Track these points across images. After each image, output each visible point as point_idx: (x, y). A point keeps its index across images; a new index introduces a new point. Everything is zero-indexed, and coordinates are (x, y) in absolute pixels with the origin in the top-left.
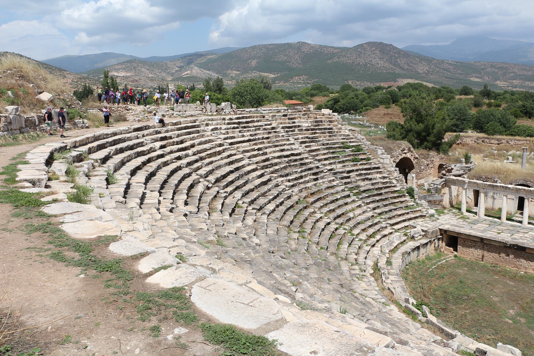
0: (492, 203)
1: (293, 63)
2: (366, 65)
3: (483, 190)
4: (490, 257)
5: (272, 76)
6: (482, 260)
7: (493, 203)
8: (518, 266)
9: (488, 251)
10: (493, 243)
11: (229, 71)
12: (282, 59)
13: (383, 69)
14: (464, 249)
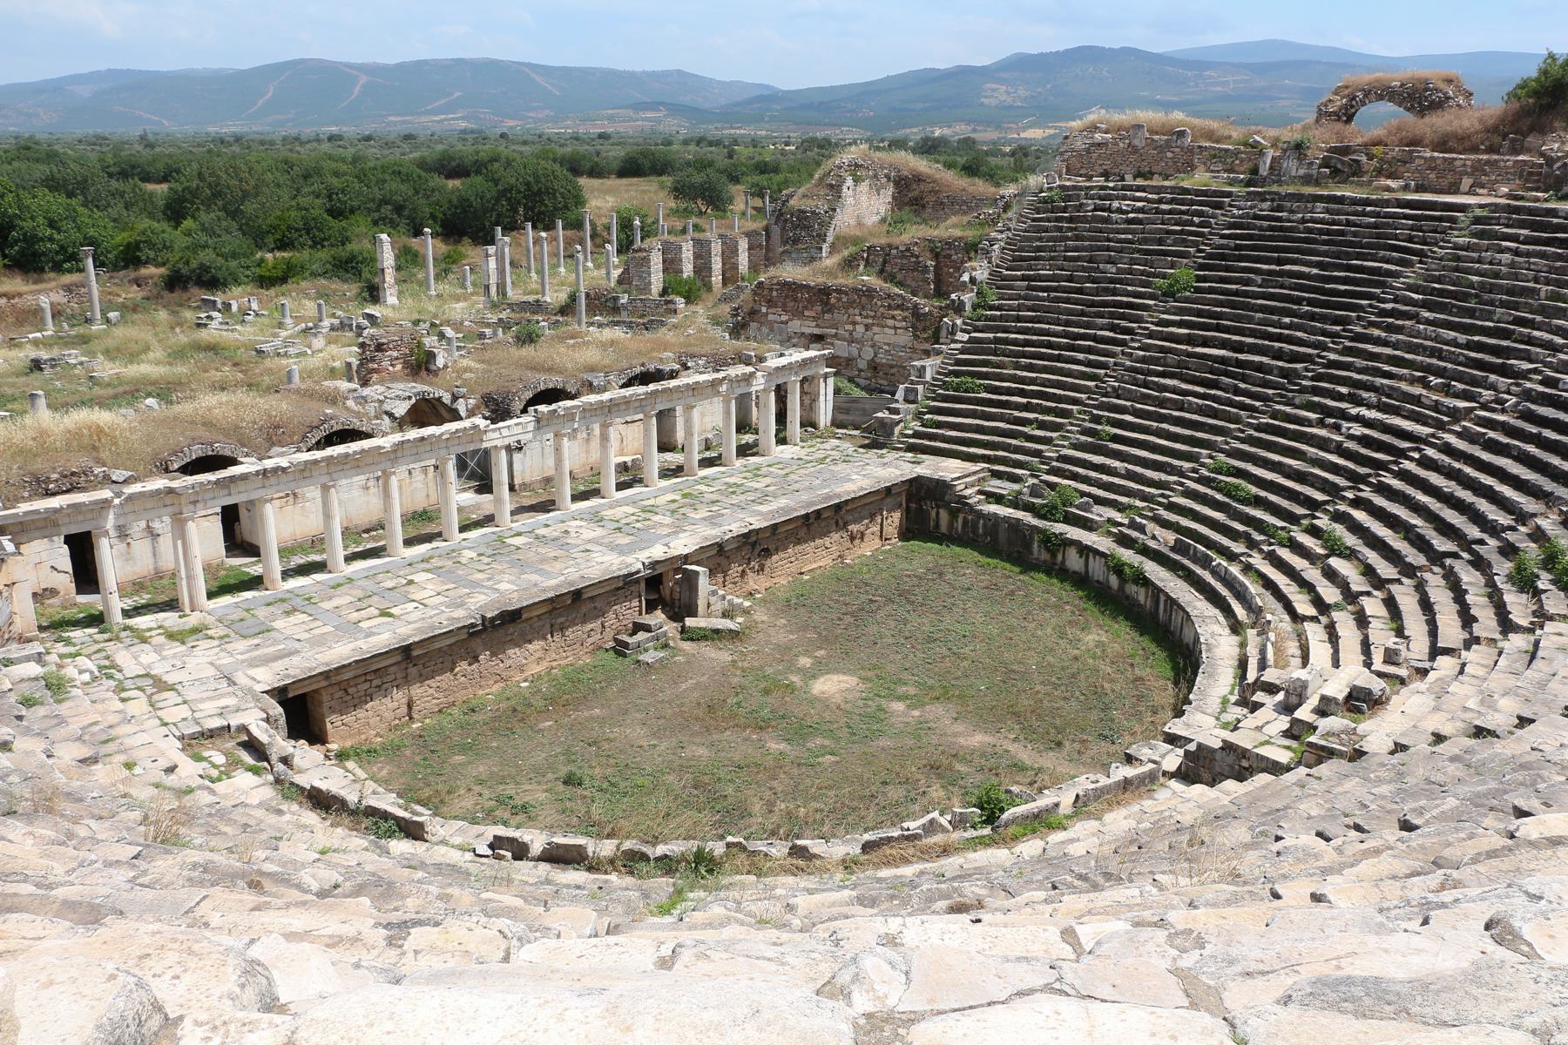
0: (150, 555)
3: (191, 507)
4: (426, 694)
6: (411, 718)
7: (155, 555)
8: (504, 674)
9: (422, 678)
10: (437, 645)
14: (348, 719)
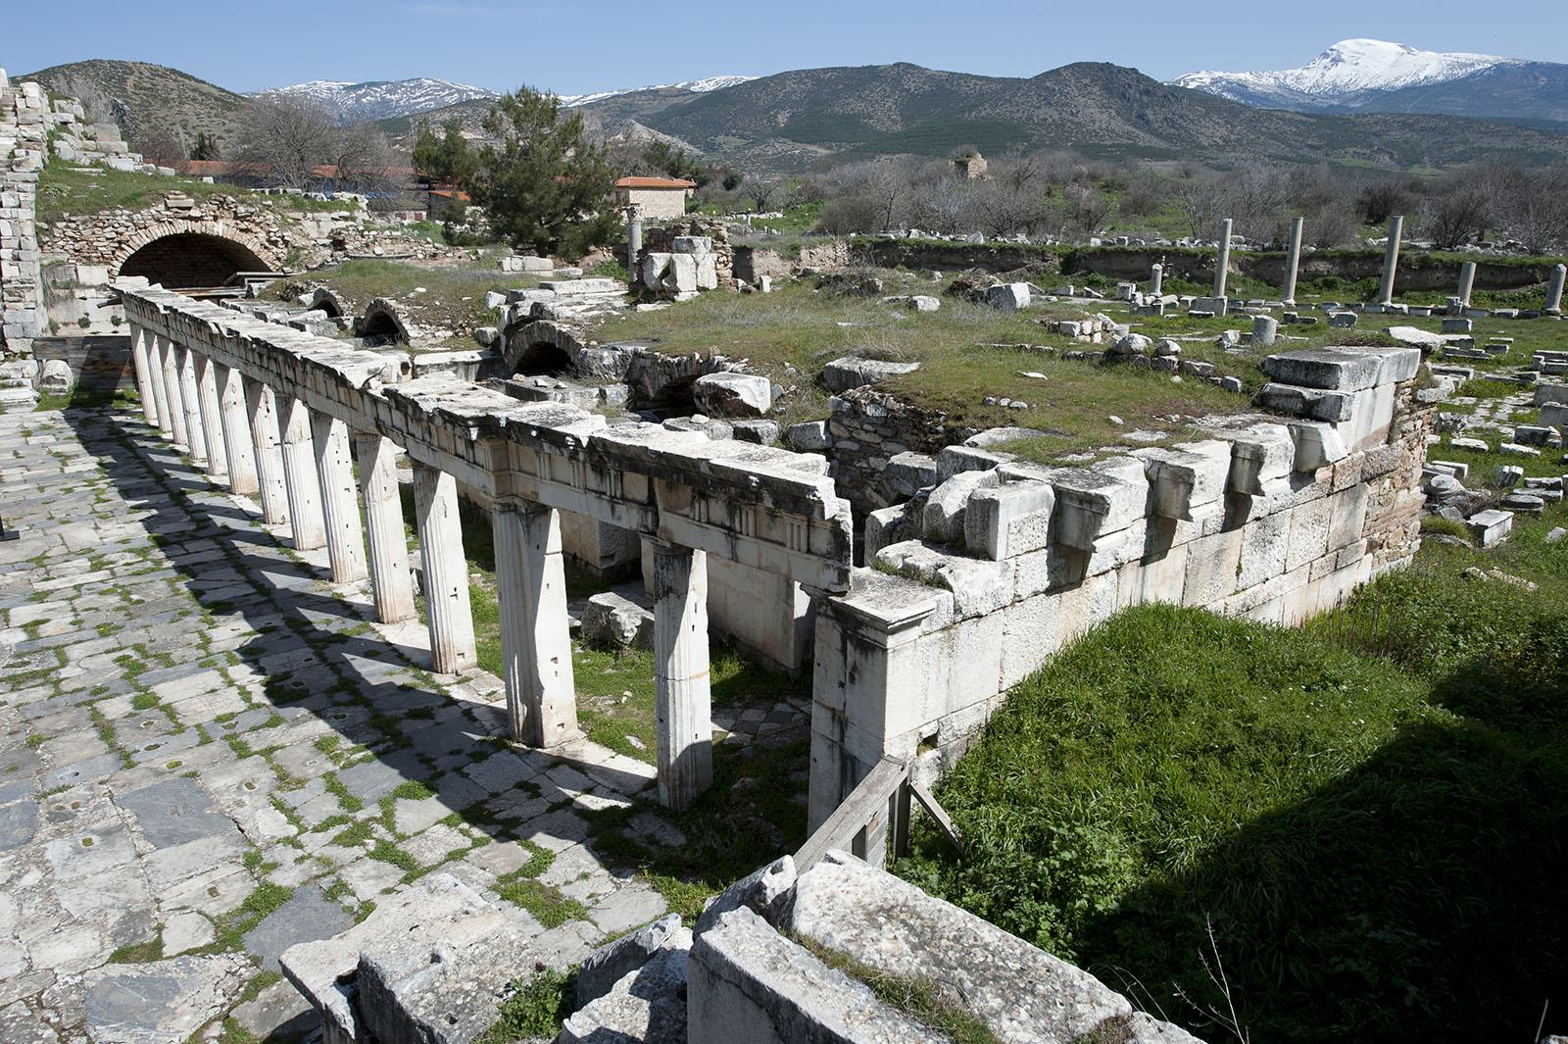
1: (878, 120)
2: (1063, 125)
5: (822, 152)
11: (721, 139)
12: (852, 109)
13: (1104, 135)
